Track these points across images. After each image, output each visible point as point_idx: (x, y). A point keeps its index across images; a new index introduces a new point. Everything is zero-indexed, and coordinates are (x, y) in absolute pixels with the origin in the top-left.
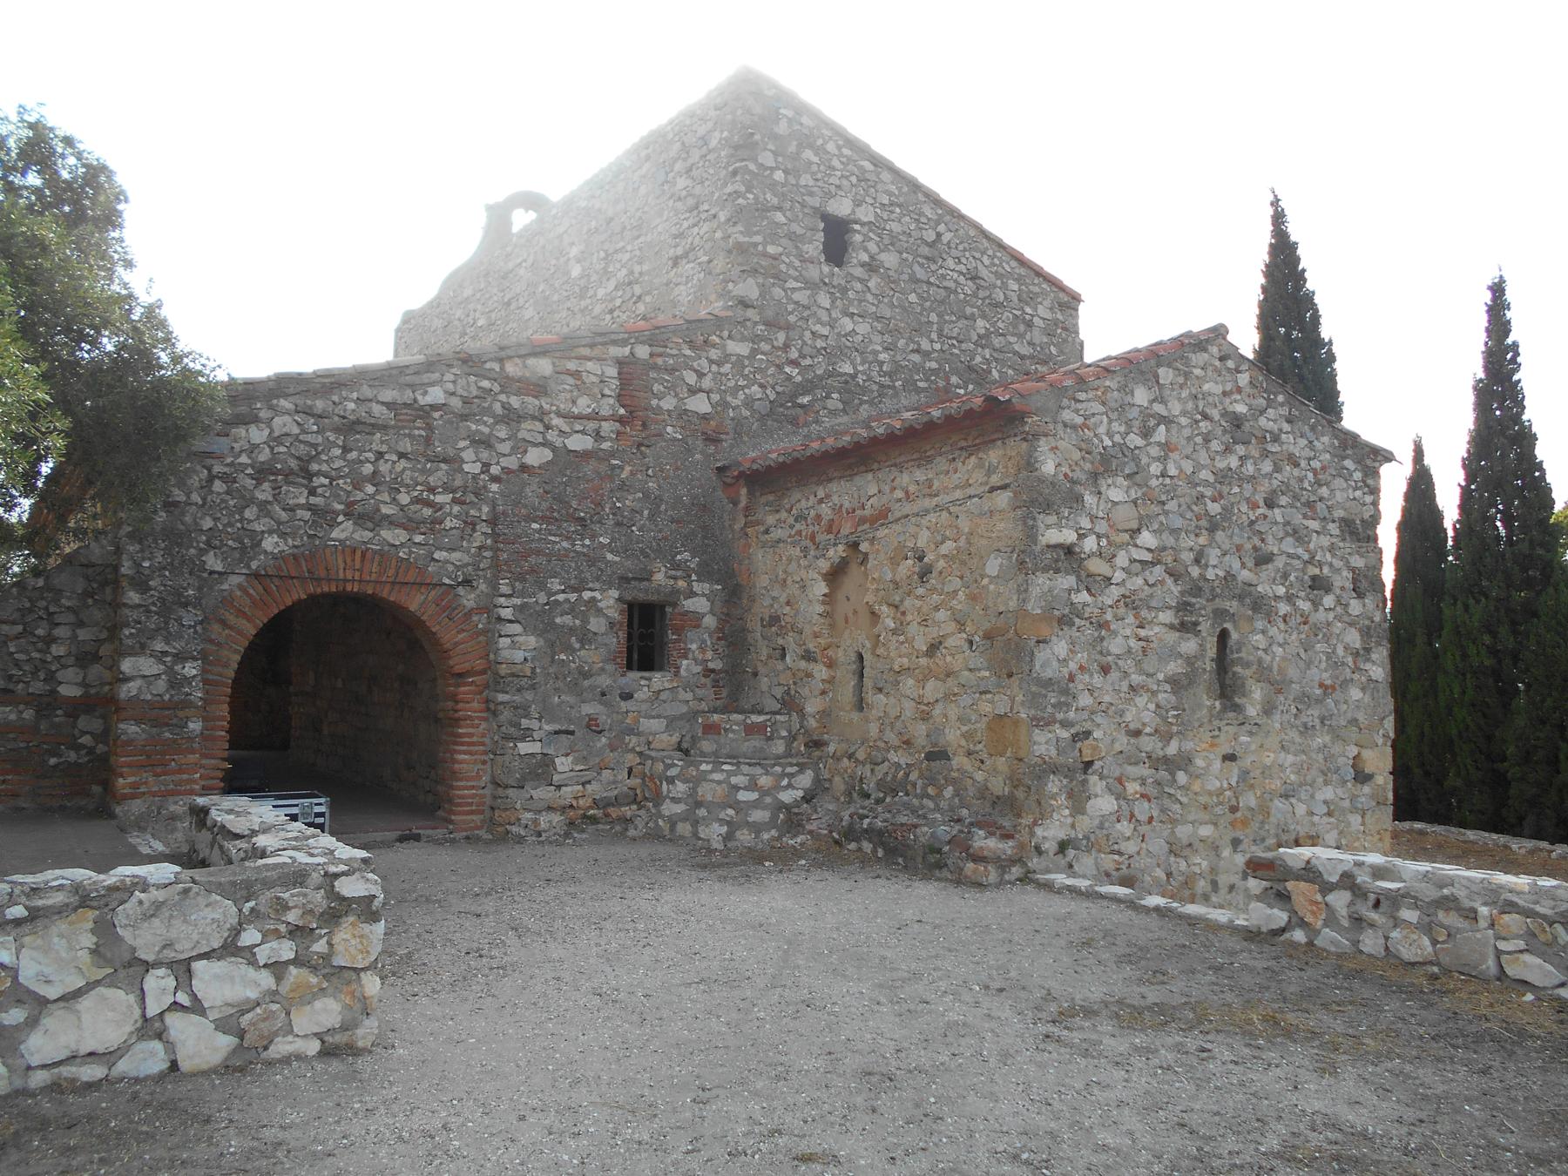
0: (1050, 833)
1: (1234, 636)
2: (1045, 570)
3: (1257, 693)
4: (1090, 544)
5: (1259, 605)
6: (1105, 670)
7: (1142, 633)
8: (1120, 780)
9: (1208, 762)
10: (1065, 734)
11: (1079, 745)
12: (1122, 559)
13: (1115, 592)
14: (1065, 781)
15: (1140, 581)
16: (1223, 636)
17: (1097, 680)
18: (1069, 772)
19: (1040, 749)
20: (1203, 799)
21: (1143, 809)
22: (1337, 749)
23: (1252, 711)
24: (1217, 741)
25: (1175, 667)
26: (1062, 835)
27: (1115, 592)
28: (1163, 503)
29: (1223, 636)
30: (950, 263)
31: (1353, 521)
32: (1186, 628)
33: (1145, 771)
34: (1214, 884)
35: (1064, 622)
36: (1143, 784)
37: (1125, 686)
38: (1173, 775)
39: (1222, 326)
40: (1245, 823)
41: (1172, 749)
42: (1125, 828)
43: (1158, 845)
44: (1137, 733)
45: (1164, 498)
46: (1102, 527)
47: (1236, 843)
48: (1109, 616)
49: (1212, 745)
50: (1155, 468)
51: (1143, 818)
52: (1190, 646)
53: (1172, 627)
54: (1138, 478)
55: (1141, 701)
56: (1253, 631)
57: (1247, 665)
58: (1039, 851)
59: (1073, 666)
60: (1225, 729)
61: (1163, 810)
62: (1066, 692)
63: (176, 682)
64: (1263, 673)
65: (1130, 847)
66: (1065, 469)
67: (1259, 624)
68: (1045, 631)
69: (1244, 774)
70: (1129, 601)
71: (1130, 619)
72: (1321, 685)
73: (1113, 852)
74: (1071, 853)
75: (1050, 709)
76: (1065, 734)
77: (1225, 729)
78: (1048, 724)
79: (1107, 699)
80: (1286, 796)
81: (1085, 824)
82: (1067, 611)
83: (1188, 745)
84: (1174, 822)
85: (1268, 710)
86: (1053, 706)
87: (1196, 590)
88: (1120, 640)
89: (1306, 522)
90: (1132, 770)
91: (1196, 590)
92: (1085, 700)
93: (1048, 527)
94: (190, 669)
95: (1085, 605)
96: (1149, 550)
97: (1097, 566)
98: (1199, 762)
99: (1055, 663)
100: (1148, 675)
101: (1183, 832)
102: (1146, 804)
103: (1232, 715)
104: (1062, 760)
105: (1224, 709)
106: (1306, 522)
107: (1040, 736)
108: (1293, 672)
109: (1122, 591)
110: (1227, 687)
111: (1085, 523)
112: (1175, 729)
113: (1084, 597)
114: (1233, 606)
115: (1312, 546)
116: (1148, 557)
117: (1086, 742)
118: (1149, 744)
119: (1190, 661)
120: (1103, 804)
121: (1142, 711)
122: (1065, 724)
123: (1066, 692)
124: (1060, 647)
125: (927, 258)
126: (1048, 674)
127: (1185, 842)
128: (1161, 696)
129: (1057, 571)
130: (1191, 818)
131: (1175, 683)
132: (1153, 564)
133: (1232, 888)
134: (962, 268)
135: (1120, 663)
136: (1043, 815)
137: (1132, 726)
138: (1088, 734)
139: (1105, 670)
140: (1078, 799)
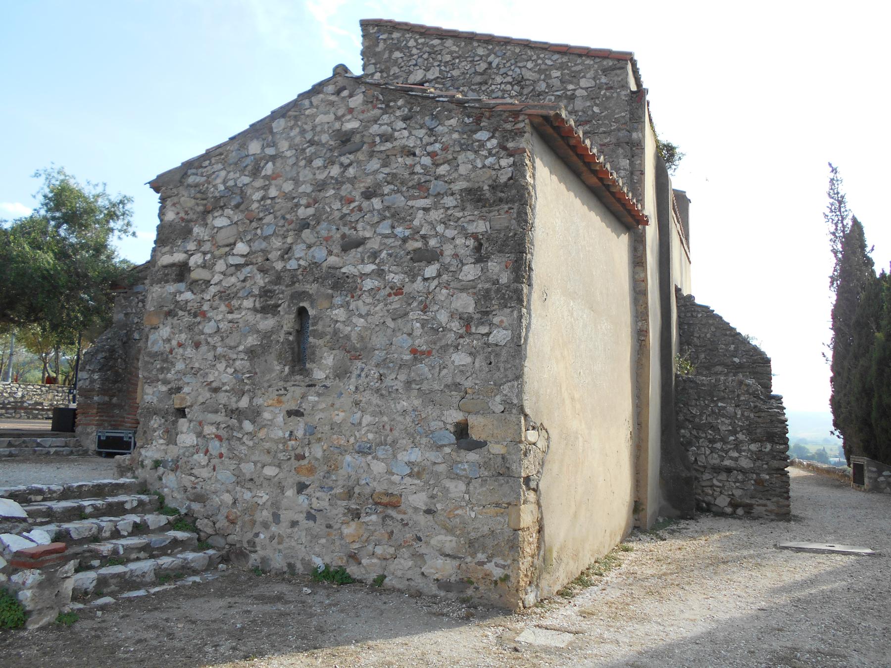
0: (149, 454)
1: (311, 312)
2: (159, 282)
3: (329, 359)
4: (196, 260)
5: (342, 284)
6: (197, 345)
7: (230, 317)
8: (200, 423)
9: (274, 415)
10: (164, 388)
11: (173, 396)
12: (220, 266)
13: (213, 290)
14: (163, 421)
15: (233, 280)
16: (302, 313)
17: (189, 352)
18: (164, 414)
19: (148, 398)
20: (267, 445)
21: (215, 446)
22: (430, 411)
23: (319, 374)
24: (284, 398)
25: (252, 340)
26: (158, 456)
27: (213, 290)
28: (261, 219)
29: (302, 313)
30: (499, 79)
31: (480, 189)
32: (269, 309)
33: (220, 418)
34: (276, 518)
35: (170, 314)
36: (217, 429)
37: (210, 356)
38: (240, 422)
39: (337, 67)
40: (311, 470)
41: (244, 403)
42: (201, 458)
43: (225, 475)
44: (216, 390)
45: (261, 215)
46: (207, 247)
47: (301, 488)
48: (205, 307)
49: (279, 402)
50: (257, 196)
51: (215, 453)
52: (267, 323)
53: (255, 310)
54: (242, 207)
55: (221, 366)
56: (332, 307)
57: (321, 336)
58: (143, 466)
59: (174, 343)
60: (291, 389)
61: (231, 449)
62: (165, 360)
63: (92, 381)
64: (338, 341)
65: (204, 473)
66: (182, 215)
67: (338, 300)
68: (155, 321)
69: (311, 430)
70: (225, 296)
71: (223, 308)
72: (414, 351)
73: (191, 474)
74: (161, 470)
75: (154, 372)
76: (164, 388)
77: (291, 389)
78: (152, 382)
79: (197, 365)
80: (361, 452)
81: (173, 452)
82: (172, 307)
83: (258, 401)
84: (241, 460)
85: (341, 373)
86: (158, 370)
87: (278, 279)
88: (212, 323)
89: (410, 203)
90: (212, 417)
91: (278, 280)
92: (180, 366)
93: (164, 254)
94: (96, 377)
95: (187, 302)
96: (242, 256)
97: (198, 274)
98: (267, 415)
99: (161, 342)
100: (231, 348)
101: (248, 468)
102: (217, 443)
103: (298, 377)
104: (161, 406)
105: (292, 372)
106: (410, 203)
107: (149, 390)
108: (378, 340)
109: (218, 288)
110: (299, 357)
111: (191, 246)
112: (247, 387)
113: (188, 295)
114: (312, 288)
115: (416, 223)
116: (241, 261)
117: (178, 395)
118: (222, 398)
119: (266, 336)
120: (187, 439)
121: (222, 375)
122: (166, 382)
123: (165, 360)
124: (165, 331)
125: (480, 84)
126: (156, 349)
127: (248, 477)
128: (238, 363)
129: (167, 282)
130: (254, 458)
131: (251, 353)
132: (246, 264)
133: (294, 524)
134: (509, 79)
135: (209, 339)
136: (148, 442)
137: (214, 385)
138: (179, 389)
139: (197, 345)
140: (171, 437)
